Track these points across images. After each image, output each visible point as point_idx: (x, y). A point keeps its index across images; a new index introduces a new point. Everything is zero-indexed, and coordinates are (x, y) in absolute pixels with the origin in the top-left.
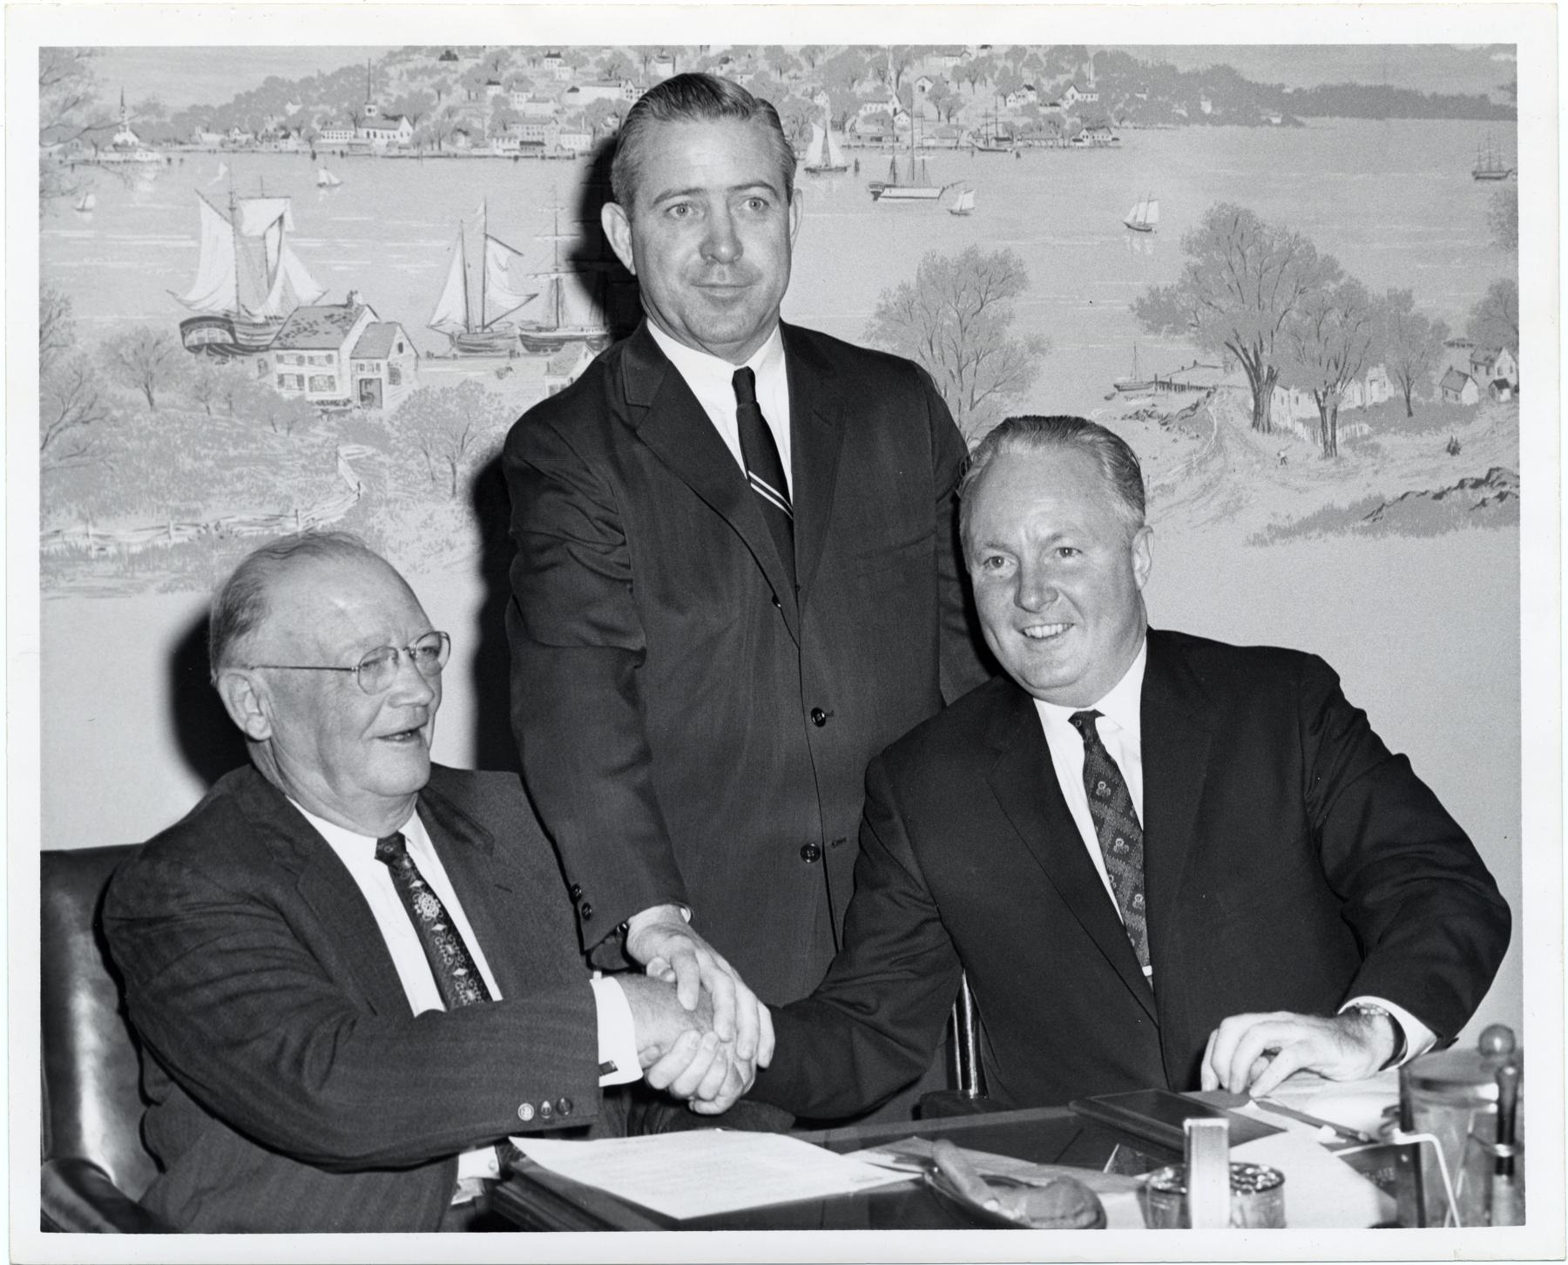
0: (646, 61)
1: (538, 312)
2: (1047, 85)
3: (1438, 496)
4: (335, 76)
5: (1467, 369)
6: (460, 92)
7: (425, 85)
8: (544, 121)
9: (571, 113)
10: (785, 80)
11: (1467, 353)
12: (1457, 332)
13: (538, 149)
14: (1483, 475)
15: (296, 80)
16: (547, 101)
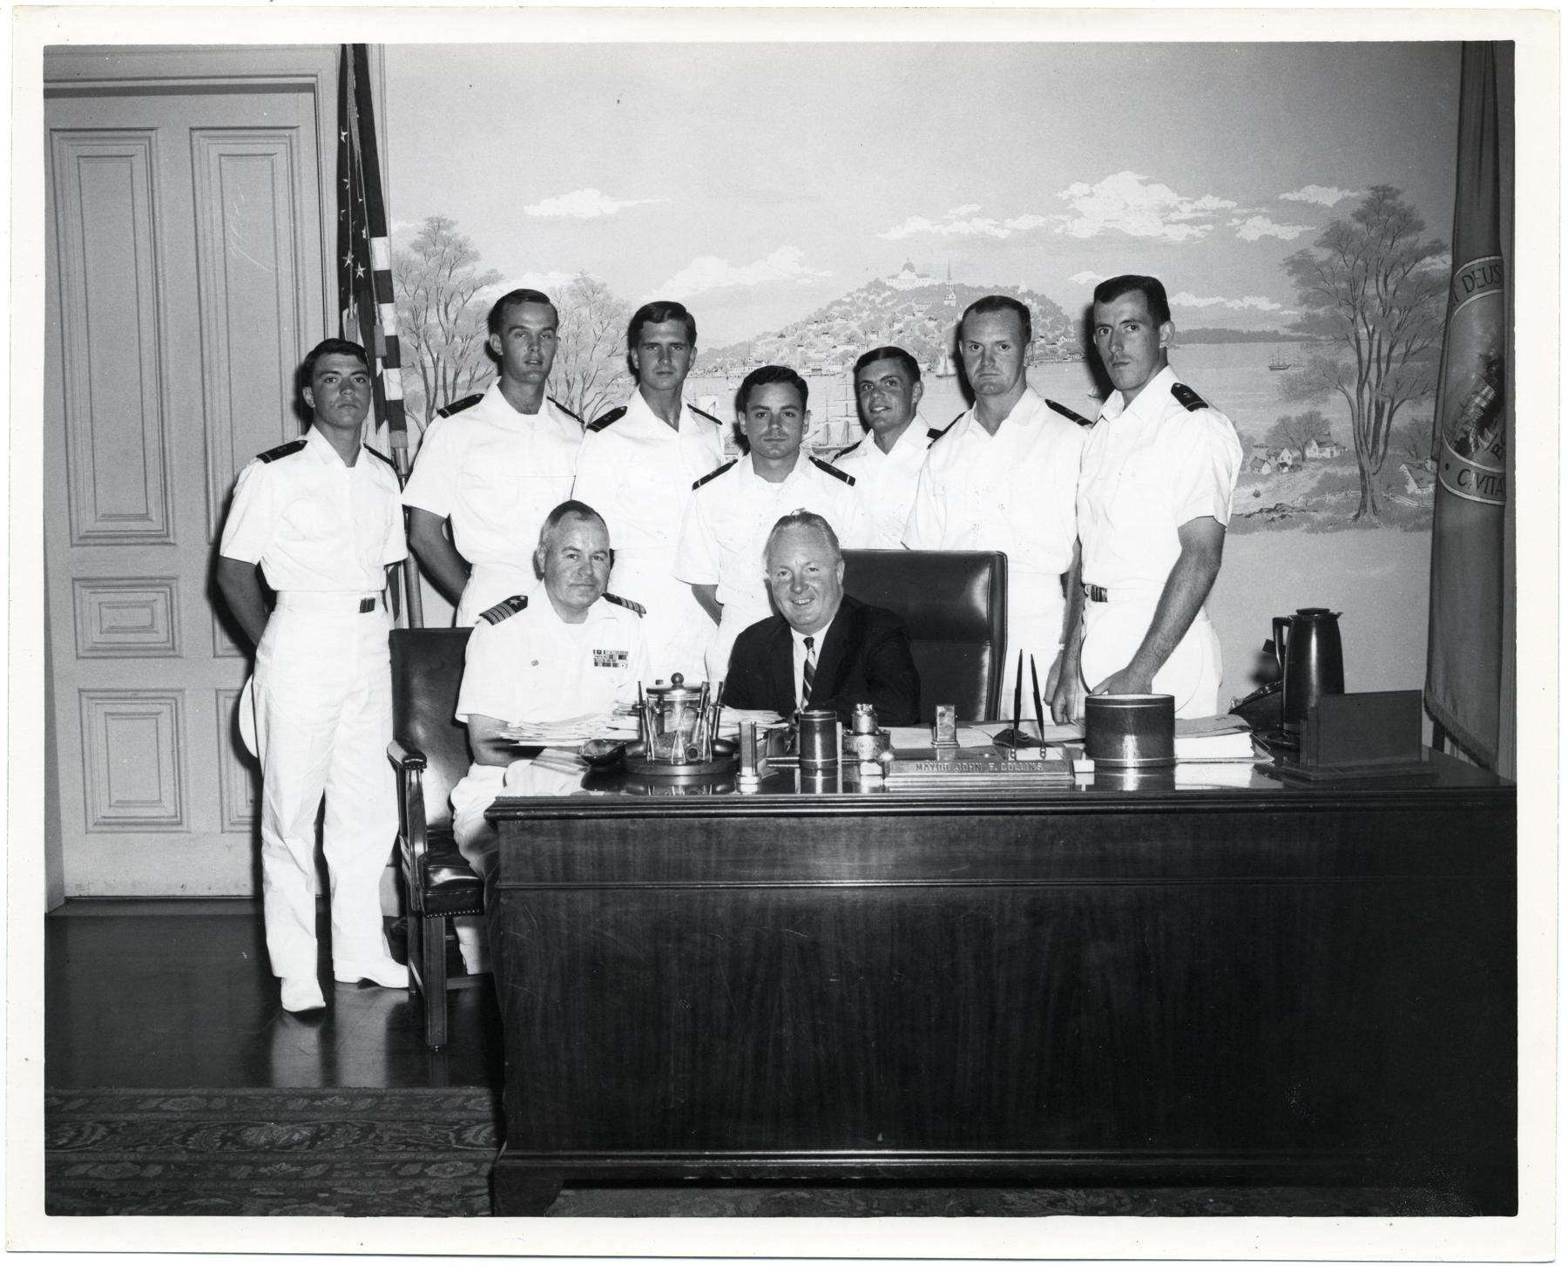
0: (865, 333)
1: (820, 438)
2: (1050, 336)
3: (1249, 516)
4: (736, 346)
5: (1265, 458)
6: (786, 350)
7: (772, 348)
8: (821, 361)
9: (833, 357)
10: (927, 339)
11: (1265, 450)
12: (1260, 440)
13: (819, 372)
14: (1272, 506)
15: (719, 347)
16: (822, 352)
